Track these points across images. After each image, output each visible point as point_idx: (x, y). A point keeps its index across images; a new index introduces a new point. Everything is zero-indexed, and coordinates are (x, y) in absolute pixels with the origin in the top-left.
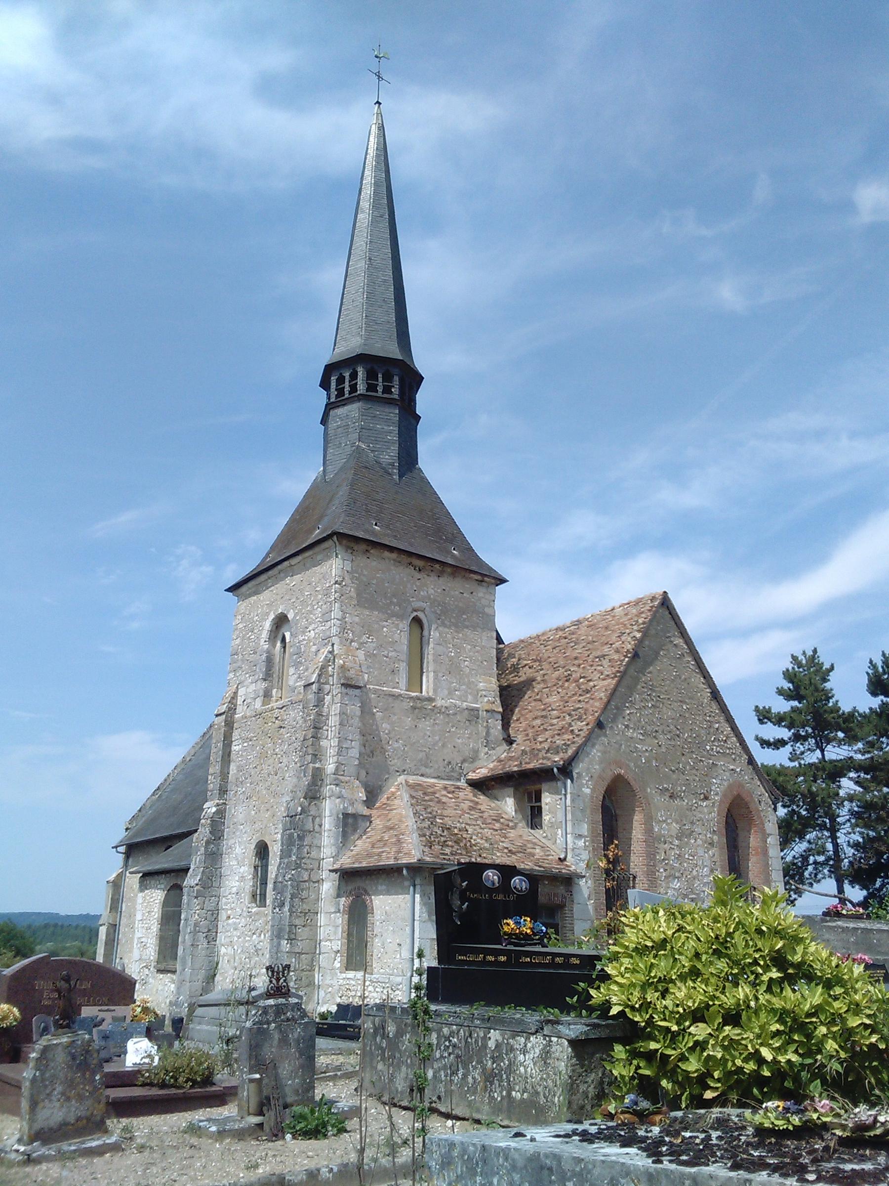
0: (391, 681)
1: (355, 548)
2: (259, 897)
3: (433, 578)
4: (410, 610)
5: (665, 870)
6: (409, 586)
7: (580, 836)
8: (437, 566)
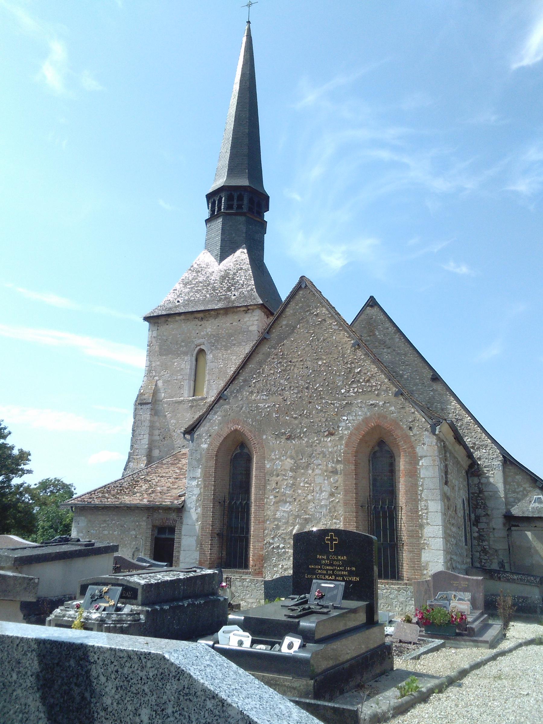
0: (179, 393)
1: (159, 322)
2: (518, 526)
3: (212, 320)
4: (193, 346)
5: (275, 497)
6: (193, 332)
7: (194, 478)
8: (212, 312)
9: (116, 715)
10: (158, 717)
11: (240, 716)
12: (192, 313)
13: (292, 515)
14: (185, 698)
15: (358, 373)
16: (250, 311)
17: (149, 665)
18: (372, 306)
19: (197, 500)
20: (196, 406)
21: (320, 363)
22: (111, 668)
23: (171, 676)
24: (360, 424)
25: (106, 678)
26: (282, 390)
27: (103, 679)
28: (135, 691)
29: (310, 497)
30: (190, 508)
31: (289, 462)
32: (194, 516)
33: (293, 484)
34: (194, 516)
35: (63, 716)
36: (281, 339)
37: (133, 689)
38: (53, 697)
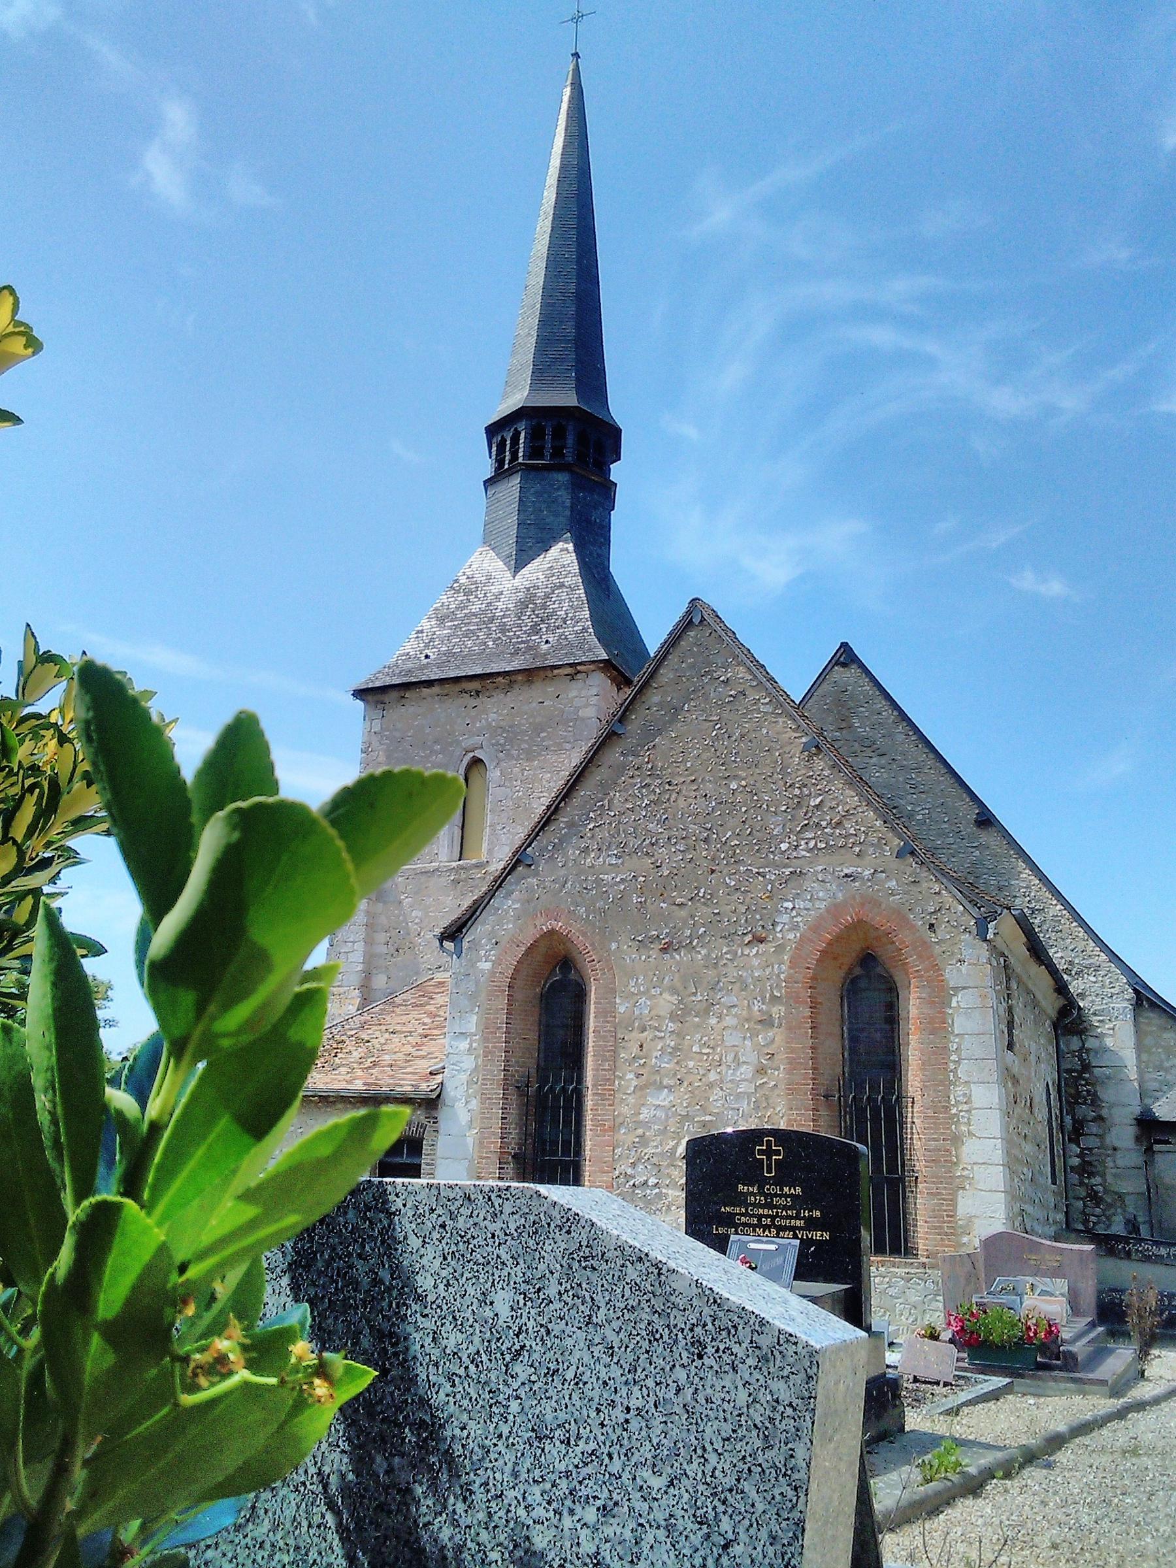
3: (499, 697)
4: (459, 752)
5: (638, 1076)
8: (500, 679)
9: (445, 1307)
10: (529, 1303)
11: (695, 1291)
12: (456, 680)
13: (675, 1114)
14: (583, 1264)
15: (817, 807)
16: (579, 676)
17: (508, 1208)
18: (844, 665)
19: (470, 1083)
20: (465, 880)
21: (734, 786)
22: (431, 1221)
23: (552, 1226)
24: (821, 917)
25: (421, 1239)
26: (653, 845)
27: (414, 1242)
28: (481, 1260)
29: (713, 1076)
30: (456, 1099)
31: (667, 1002)
32: (463, 1117)
33: (676, 1049)
34: (463, 1117)
35: (336, 1318)
36: (649, 734)
37: (477, 1256)
38: (314, 1284)
